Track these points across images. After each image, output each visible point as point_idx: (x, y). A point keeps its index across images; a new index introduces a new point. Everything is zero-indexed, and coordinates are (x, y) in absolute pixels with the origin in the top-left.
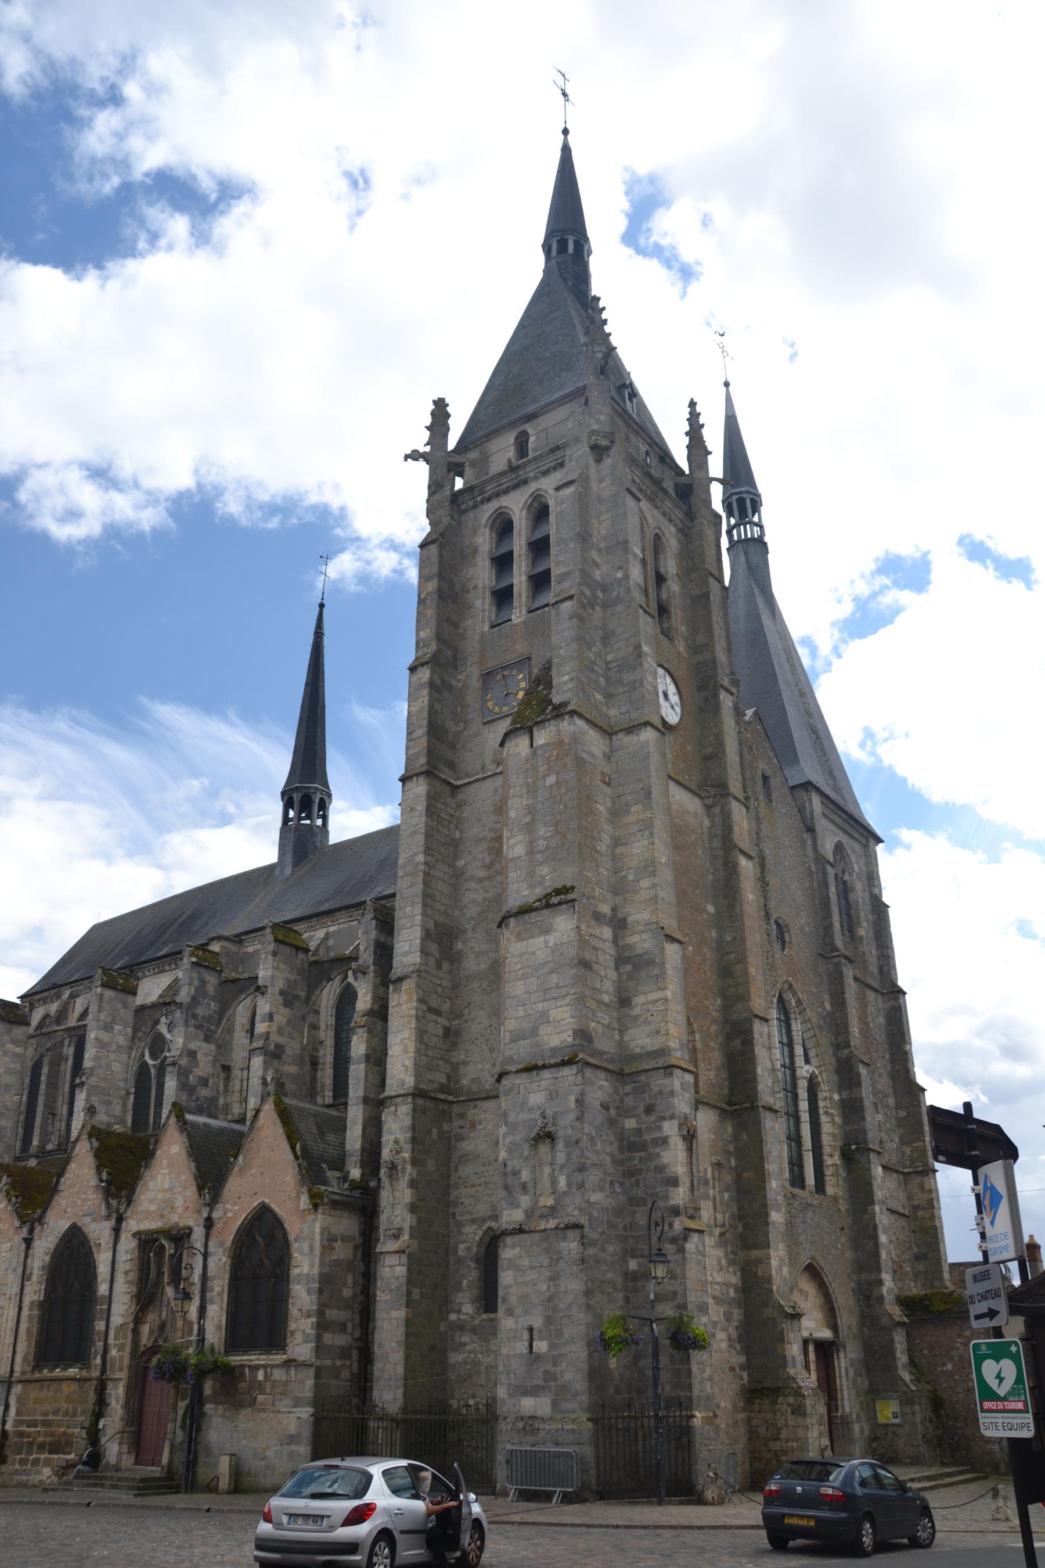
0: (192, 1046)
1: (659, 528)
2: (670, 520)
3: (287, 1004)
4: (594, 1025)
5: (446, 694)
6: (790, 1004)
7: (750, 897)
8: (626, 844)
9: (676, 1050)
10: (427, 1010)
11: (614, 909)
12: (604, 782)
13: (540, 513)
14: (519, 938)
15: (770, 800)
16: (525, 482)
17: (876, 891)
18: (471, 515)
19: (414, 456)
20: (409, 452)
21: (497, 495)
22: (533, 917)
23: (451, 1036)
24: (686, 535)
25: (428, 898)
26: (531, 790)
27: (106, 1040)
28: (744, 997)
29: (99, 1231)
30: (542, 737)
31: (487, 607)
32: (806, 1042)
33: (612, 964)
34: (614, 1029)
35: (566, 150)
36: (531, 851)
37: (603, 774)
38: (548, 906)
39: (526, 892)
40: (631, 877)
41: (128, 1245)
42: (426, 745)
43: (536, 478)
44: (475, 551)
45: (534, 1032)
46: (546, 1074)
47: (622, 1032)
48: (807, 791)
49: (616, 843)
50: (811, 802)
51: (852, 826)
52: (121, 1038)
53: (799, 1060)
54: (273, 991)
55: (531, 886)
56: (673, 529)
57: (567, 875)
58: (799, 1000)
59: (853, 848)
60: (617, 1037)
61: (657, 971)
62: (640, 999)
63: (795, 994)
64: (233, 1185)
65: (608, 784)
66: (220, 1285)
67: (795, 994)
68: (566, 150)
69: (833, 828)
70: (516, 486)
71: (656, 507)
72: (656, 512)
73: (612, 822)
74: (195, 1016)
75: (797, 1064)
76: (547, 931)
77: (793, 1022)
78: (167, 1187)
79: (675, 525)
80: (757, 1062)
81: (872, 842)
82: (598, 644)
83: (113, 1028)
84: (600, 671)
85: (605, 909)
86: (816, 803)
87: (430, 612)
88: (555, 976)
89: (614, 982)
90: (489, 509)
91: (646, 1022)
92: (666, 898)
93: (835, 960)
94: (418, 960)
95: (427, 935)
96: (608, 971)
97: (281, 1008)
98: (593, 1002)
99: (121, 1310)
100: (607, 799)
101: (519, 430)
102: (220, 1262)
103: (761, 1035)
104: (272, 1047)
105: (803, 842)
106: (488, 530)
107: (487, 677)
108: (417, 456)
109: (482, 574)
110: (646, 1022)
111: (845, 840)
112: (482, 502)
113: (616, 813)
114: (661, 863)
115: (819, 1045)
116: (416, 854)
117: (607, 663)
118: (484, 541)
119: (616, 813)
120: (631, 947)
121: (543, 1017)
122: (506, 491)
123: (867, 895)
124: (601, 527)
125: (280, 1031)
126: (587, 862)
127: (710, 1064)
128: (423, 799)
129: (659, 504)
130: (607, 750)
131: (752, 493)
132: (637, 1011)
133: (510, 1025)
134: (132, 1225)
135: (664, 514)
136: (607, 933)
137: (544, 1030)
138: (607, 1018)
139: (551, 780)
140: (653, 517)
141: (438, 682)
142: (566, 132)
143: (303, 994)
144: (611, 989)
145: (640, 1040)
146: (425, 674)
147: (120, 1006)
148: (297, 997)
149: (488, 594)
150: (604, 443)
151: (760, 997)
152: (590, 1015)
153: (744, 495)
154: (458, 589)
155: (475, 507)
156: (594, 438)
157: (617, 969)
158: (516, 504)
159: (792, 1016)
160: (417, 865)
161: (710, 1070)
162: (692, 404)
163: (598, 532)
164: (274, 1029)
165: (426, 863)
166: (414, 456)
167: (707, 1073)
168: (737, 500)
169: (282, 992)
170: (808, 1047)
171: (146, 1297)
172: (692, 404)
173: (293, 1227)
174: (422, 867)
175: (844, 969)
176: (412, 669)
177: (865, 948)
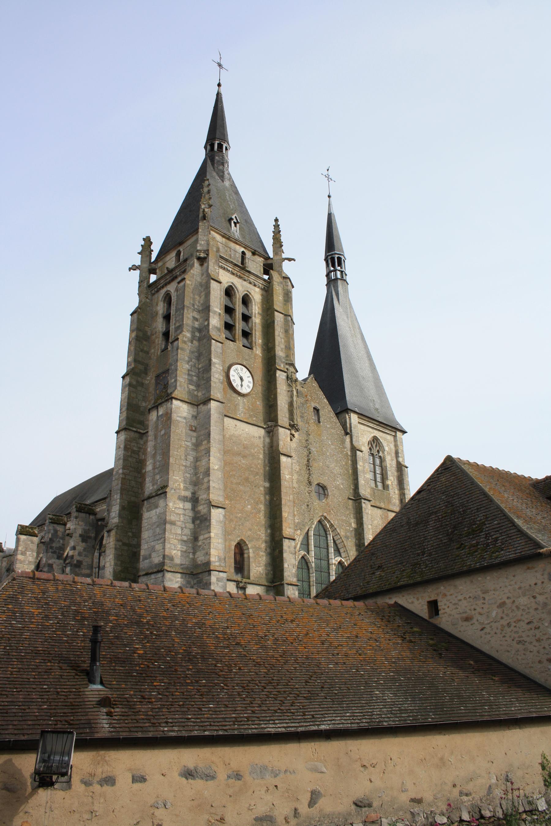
0: (50, 562)
1: (248, 291)
2: (255, 285)
3: (83, 541)
4: (175, 552)
5: (139, 388)
6: (327, 527)
7: (287, 477)
8: (200, 460)
9: (215, 562)
11: (194, 493)
12: (191, 430)
14: (148, 511)
15: (319, 422)
16: (176, 277)
17: (400, 460)
18: (156, 296)
19: (133, 268)
20: (131, 266)
21: (166, 285)
22: (152, 500)
24: (266, 291)
26: (156, 438)
27: (22, 559)
28: (280, 529)
30: (161, 411)
31: (160, 342)
32: (338, 545)
33: (190, 521)
34: (189, 553)
35: (219, 95)
36: (154, 469)
37: (191, 426)
38: (157, 495)
39: (151, 488)
40: (201, 477)
42: (126, 415)
43: (180, 275)
44: (157, 314)
45: (150, 556)
46: (153, 576)
47: (194, 553)
48: (348, 413)
50: (350, 418)
51: (383, 427)
52: (30, 558)
53: (332, 555)
54: (76, 535)
55: (153, 485)
56: (257, 290)
58: (332, 524)
59: (386, 439)
60: (191, 556)
61: (208, 524)
62: (201, 538)
63: (329, 522)
65: (194, 431)
67: (329, 522)
68: (219, 95)
69: (370, 429)
70: (173, 280)
71: (245, 280)
72: (245, 283)
73: (196, 450)
74: (52, 548)
75: (330, 558)
76: (157, 507)
77: (328, 536)
79: (259, 287)
80: (284, 561)
81: (399, 434)
82: (193, 360)
83: (26, 553)
84: (194, 374)
85: (188, 494)
86: (354, 418)
87: (132, 348)
88: (158, 529)
89: (190, 529)
90: (163, 291)
91: (203, 549)
92: (216, 487)
93: (359, 501)
94: (117, 521)
96: (187, 525)
97: (80, 543)
98: (176, 541)
100: (193, 439)
101: (177, 250)
103: (289, 547)
104: (75, 562)
105: (343, 442)
106: (162, 303)
108: (134, 268)
109: (159, 325)
110: (203, 549)
111: (378, 434)
112: (160, 289)
114: (214, 469)
115: (345, 546)
116: (119, 469)
117: (199, 369)
120: (199, 512)
121: (153, 549)
122: (169, 283)
123: (394, 463)
125: (80, 554)
126: (175, 472)
127: (260, 564)
128: (123, 442)
129: (246, 278)
130: (195, 414)
131: (338, 254)
132: (200, 543)
133: (142, 553)
135: (250, 283)
136: (188, 505)
137: (154, 555)
138: (185, 548)
139: (163, 432)
140: (242, 286)
141: (134, 383)
142: (219, 85)
143: (93, 535)
144: (189, 533)
145: (200, 558)
146: (128, 380)
147: (29, 543)
148: (90, 537)
149: (161, 335)
150: (202, 255)
151: (290, 528)
152: (173, 547)
153: (334, 256)
154: (149, 334)
155: (158, 291)
156: (198, 254)
157: (193, 522)
159: (328, 533)
160: (120, 474)
161: (260, 566)
162: (276, 220)
163: (199, 302)
164: (76, 553)
165: (123, 473)
166: (133, 268)
167: (257, 568)
168: (331, 258)
169: (81, 536)
170: (339, 547)
172: (276, 220)
174: (121, 476)
175: (364, 505)
176: (123, 377)
177: (391, 491)
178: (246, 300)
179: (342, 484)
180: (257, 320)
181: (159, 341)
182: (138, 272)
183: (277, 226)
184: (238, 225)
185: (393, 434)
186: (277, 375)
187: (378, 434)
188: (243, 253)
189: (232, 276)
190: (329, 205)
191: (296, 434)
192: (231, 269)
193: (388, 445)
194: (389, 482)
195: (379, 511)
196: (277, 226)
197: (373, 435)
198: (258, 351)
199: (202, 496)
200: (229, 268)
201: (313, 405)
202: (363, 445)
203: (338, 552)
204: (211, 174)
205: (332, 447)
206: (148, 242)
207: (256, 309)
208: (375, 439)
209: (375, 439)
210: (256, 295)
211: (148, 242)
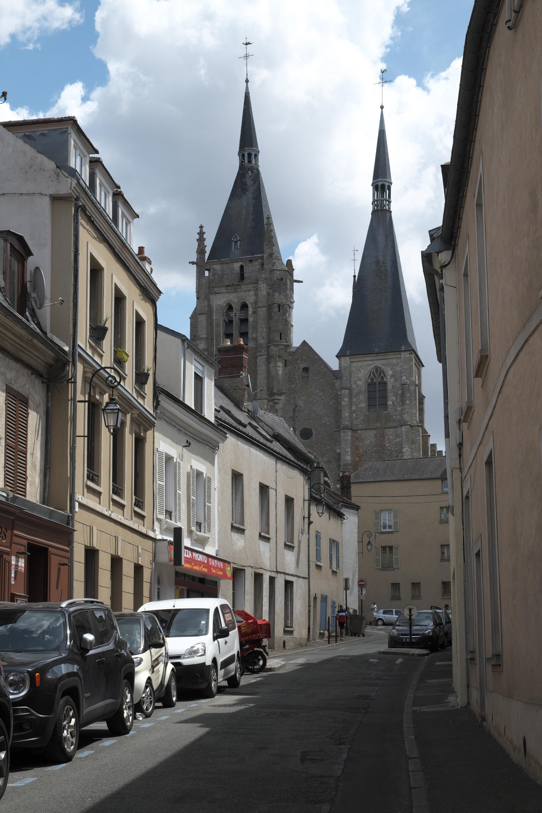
63: (312, 454)
69: (370, 362)
72: (240, 294)
178: (244, 306)
179: (329, 421)
184: (239, 242)
185: (399, 356)
186: (258, 361)
187: (379, 363)
188: (242, 267)
189: (229, 294)
191: (282, 398)
192: (225, 291)
193: (391, 369)
194: (390, 403)
195: (374, 432)
197: (372, 366)
200: (223, 291)
201: (302, 366)
202: (360, 379)
205: (320, 394)
208: (377, 369)
209: (377, 369)
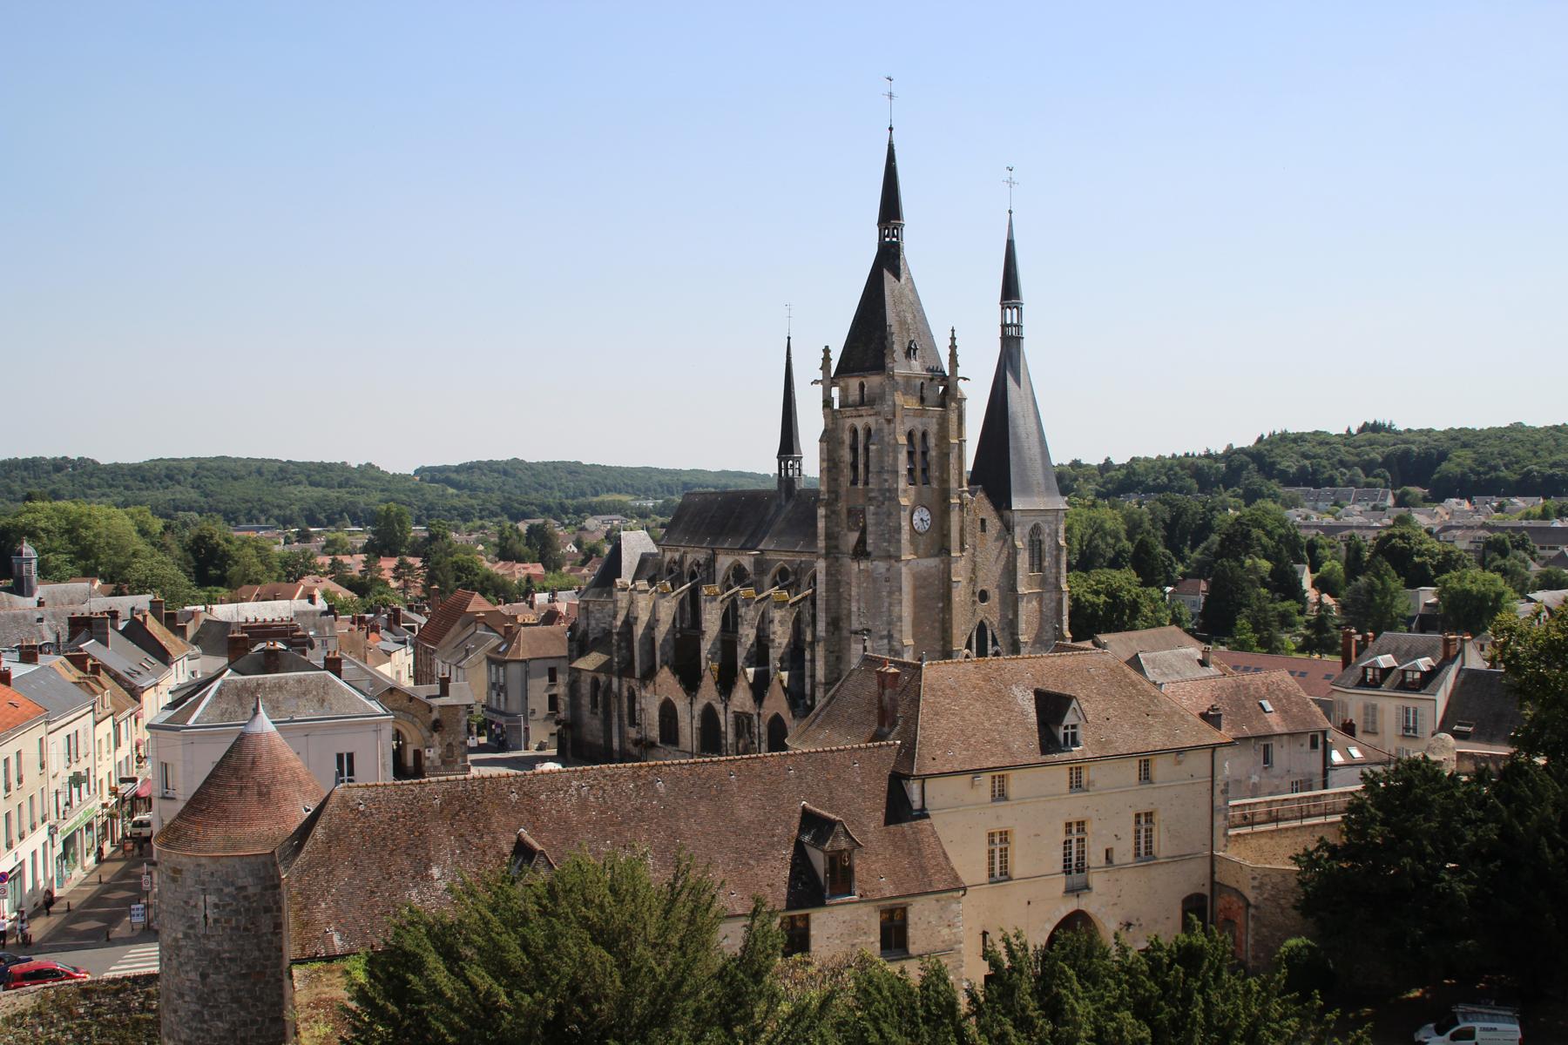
10: (829, 652)
13: (868, 432)
19: (816, 382)
23: (839, 659)
25: (827, 610)
29: (719, 707)
41: (730, 716)
49: (891, 604)
57: (870, 625)
64: (766, 703)
66: (765, 737)
78: (742, 697)
95: (828, 624)
99: (731, 738)
102: (764, 729)
107: (849, 512)
109: (847, 455)
113: (890, 593)
118: (847, 437)
119: (890, 593)
124: (889, 460)
134: (731, 708)
158: (860, 424)
166: (816, 382)
171: (738, 735)
173: (787, 723)
178: (924, 435)
180: (933, 453)
181: (847, 472)
182: (820, 386)
183: (953, 339)
190: (1010, 225)
196: (953, 339)
198: (935, 485)
199: (896, 635)
203: (995, 643)
204: (888, 276)
206: (827, 351)
207: (932, 441)
210: (933, 428)
211: (827, 351)
